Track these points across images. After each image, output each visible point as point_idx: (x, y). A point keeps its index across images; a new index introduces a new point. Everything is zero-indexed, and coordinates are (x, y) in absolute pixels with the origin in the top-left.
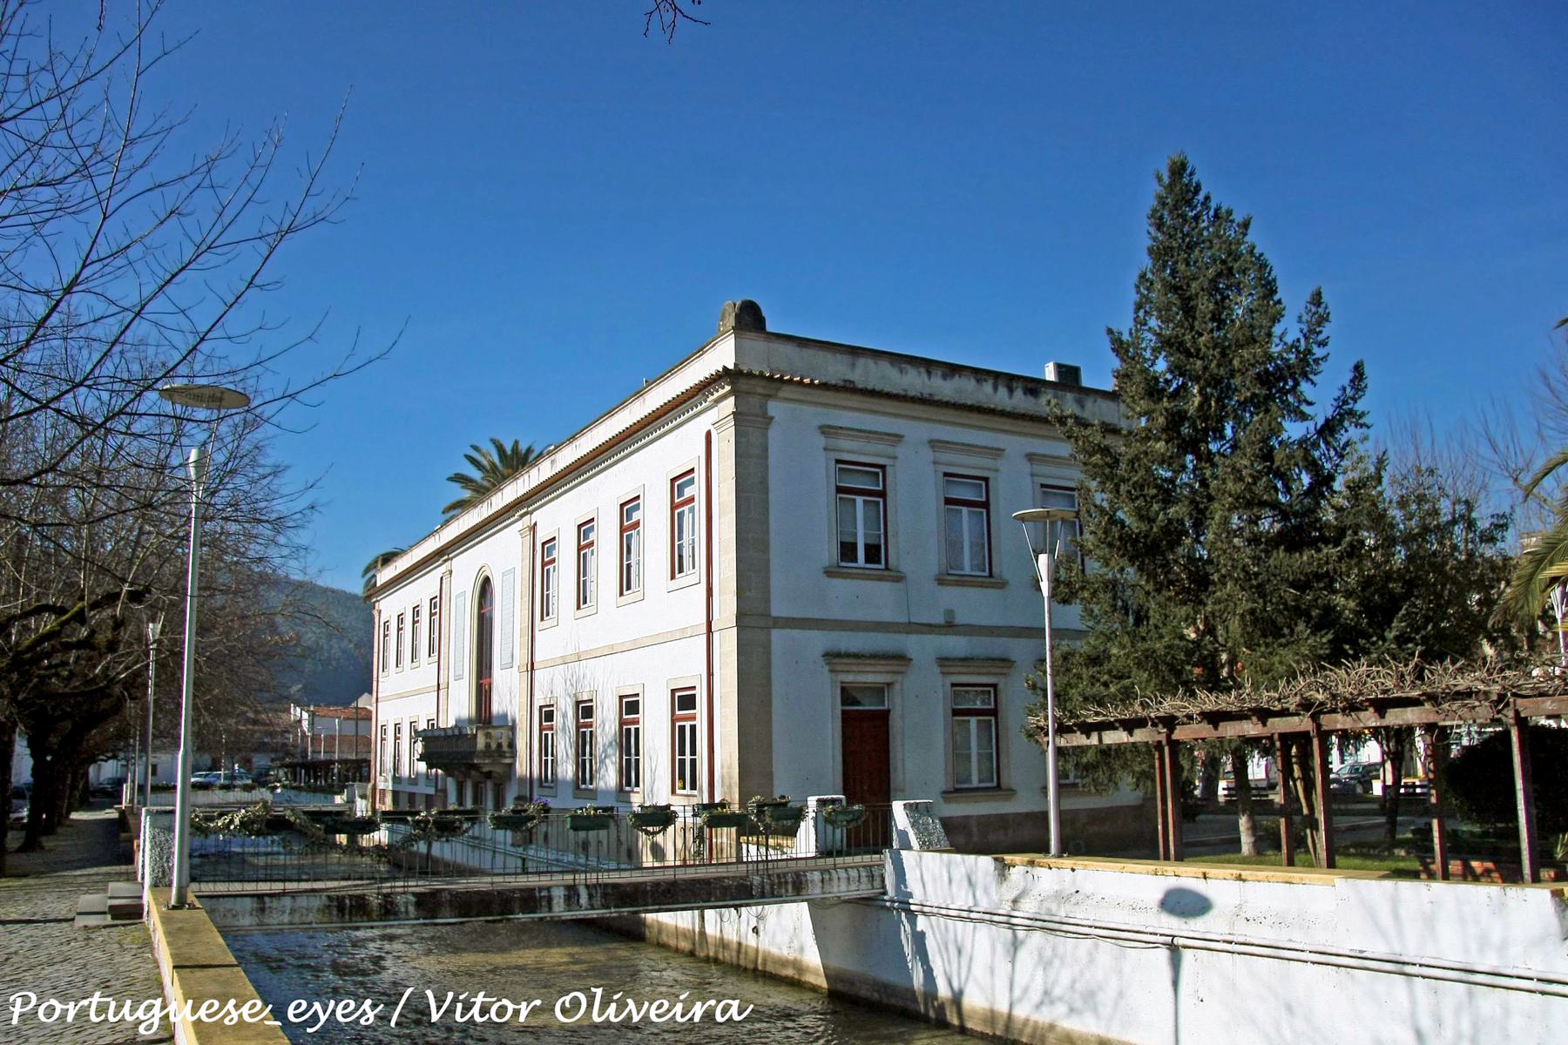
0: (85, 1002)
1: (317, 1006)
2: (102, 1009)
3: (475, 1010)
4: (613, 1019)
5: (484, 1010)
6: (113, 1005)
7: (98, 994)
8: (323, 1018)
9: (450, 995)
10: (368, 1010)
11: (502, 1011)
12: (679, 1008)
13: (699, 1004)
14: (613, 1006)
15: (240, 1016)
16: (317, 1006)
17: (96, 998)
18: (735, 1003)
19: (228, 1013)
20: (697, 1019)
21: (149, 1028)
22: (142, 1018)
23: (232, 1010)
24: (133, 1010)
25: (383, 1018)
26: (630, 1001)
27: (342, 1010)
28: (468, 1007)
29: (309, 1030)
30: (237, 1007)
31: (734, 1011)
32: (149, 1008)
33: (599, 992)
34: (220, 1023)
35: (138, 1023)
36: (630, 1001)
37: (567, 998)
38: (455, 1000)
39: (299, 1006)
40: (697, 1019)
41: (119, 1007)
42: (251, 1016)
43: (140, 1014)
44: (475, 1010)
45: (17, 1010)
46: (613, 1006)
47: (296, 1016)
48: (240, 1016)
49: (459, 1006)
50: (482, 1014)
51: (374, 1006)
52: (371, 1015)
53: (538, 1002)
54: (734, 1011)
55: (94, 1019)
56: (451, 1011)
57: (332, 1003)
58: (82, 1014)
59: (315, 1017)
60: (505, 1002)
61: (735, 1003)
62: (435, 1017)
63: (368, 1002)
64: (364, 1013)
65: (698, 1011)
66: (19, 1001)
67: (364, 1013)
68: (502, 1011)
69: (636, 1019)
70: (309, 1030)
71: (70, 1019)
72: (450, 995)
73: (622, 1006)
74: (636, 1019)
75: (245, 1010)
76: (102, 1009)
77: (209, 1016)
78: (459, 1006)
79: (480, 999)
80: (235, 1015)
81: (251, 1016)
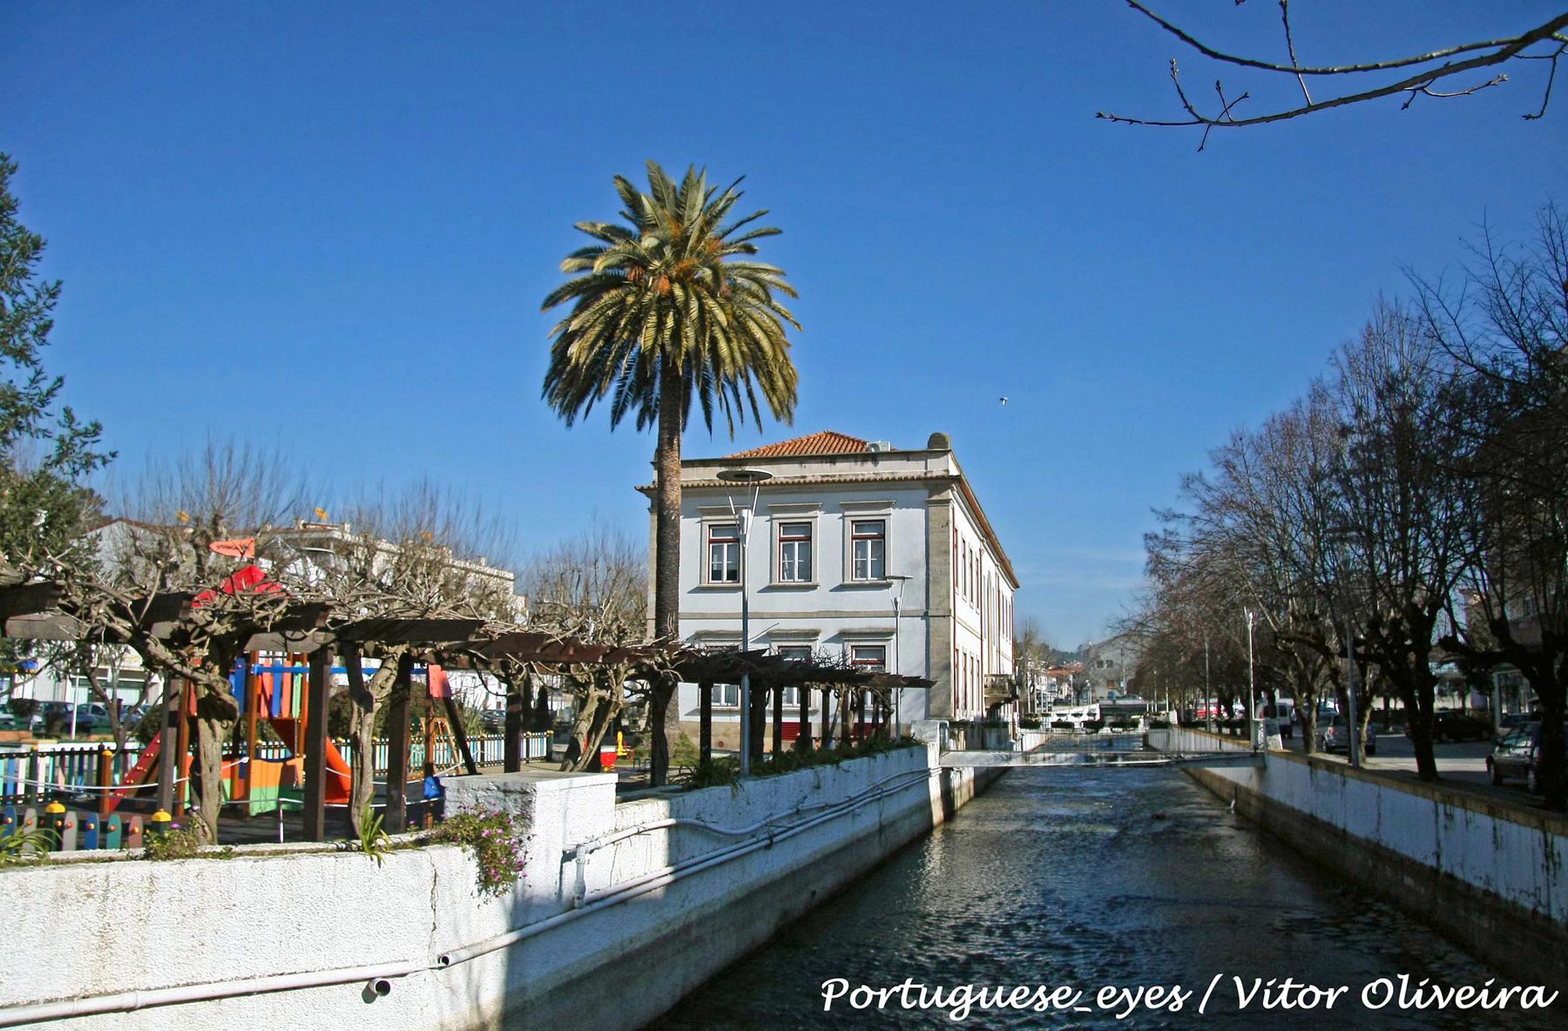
0: (897, 989)
1: (1126, 992)
3: (1283, 997)
5: (1293, 995)
8: (1132, 1005)
9: (1258, 981)
10: (1177, 997)
11: (1309, 998)
12: (1485, 994)
13: (1504, 990)
14: (1419, 993)
16: (1126, 992)
17: (908, 985)
20: (1502, 1006)
21: (960, 1014)
22: (954, 1004)
23: (1043, 997)
25: (1190, 1005)
26: (1436, 988)
27: (1151, 997)
28: (1276, 993)
29: (1119, 1017)
30: (1047, 993)
31: (1539, 997)
33: (1405, 978)
34: (1030, 1010)
35: (950, 1008)
36: (1436, 988)
37: (1374, 985)
38: (1263, 986)
40: (1502, 1006)
41: (929, 997)
42: (1061, 1002)
43: (951, 1000)
44: (1283, 997)
45: (829, 997)
46: (1419, 993)
49: (1267, 992)
51: (1181, 994)
52: (1180, 1002)
53: (1345, 989)
54: (1539, 997)
55: (905, 1005)
57: (1141, 989)
58: (894, 1000)
59: (1124, 1006)
60: (1313, 988)
61: (1540, 990)
62: (1243, 1004)
63: (1177, 988)
65: (1503, 997)
66: (831, 988)
67: (1173, 1000)
68: (1309, 998)
69: (1442, 1005)
71: (881, 1005)
72: (1258, 981)
73: (1428, 992)
75: (1055, 996)
76: (914, 994)
78: (1267, 992)
79: (1288, 985)
80: (1045, 1001)
81: (1061, 1002)
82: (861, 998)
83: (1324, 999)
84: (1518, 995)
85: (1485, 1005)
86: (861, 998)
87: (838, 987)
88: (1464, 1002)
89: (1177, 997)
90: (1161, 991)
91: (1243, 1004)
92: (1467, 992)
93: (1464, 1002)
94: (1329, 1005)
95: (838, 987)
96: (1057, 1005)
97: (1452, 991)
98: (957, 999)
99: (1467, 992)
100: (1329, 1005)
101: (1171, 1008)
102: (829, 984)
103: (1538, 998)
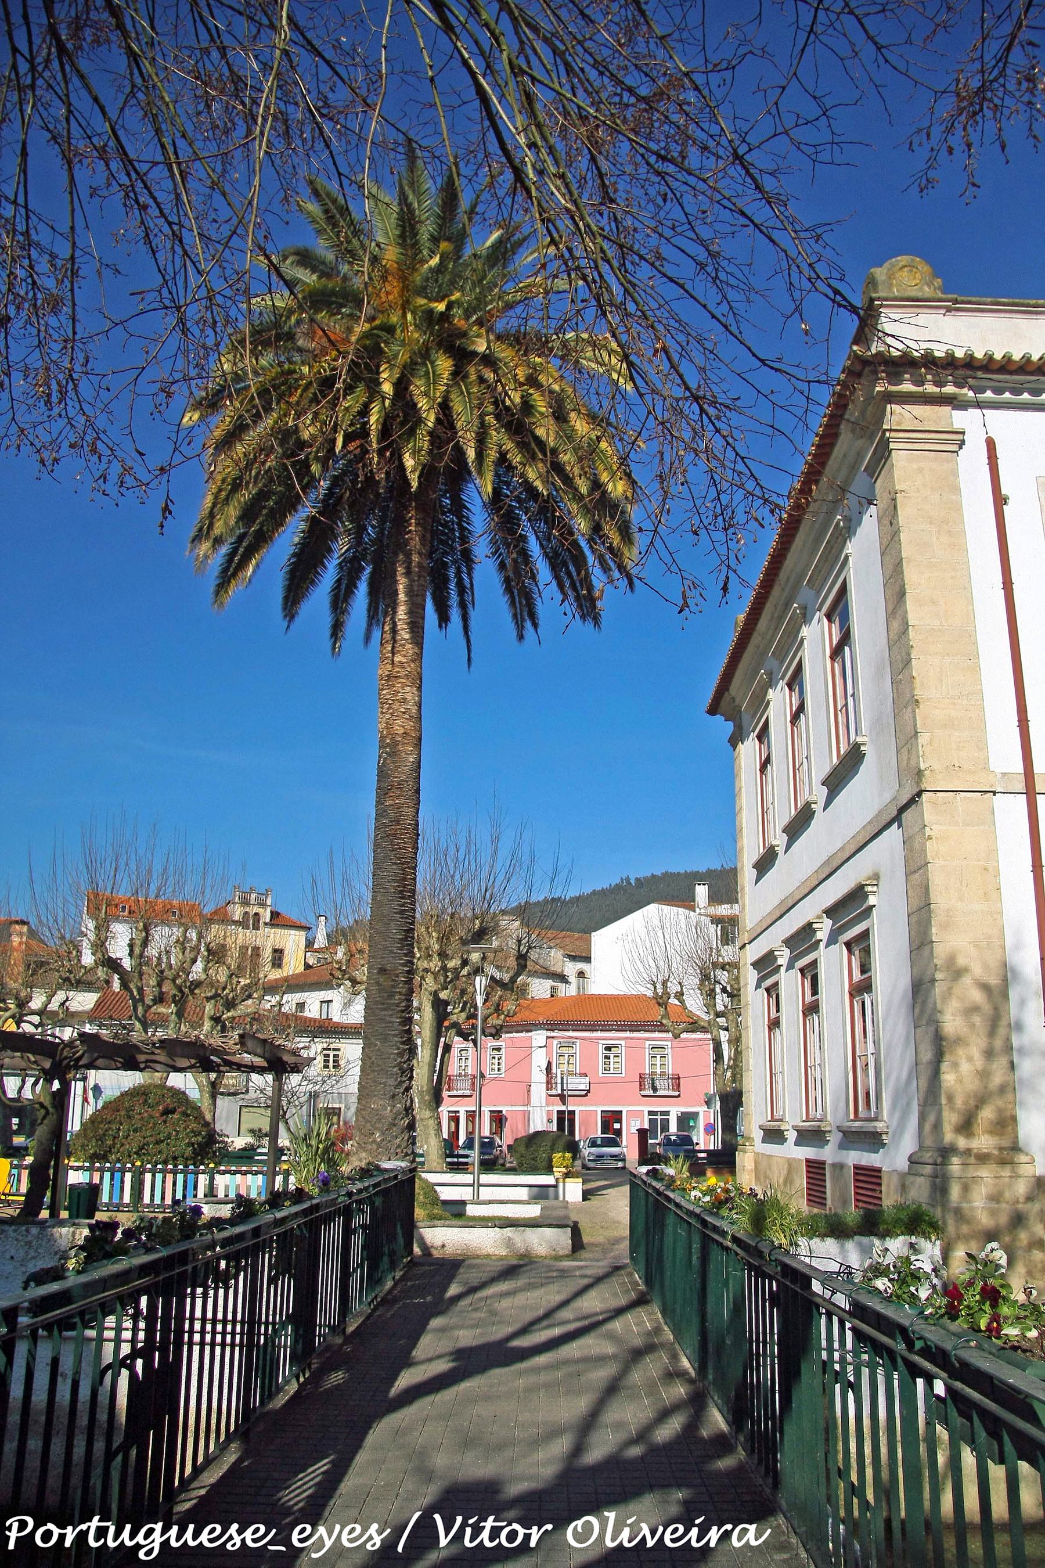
0: (84, 1527)
2: (101, 1533)
3: (485, 1535)
4: (626, 1544)
5: (495, 1533)
7: (97, 1518)
8: (328, 1543)
9: (459, 1519)
10: (375, 1535)
11: (512, 1536)
12: (694, 1532)
13: (715, 1529)
15: (243, 1540)
17: (95, 1522)
18: (752, 1528)
20: (712, 1544)
21: (148, 1553)
22: (142, 1542)
23: (235, 1535)
24: (133, 1535)
26: (644, 1526)
28: (477, 1531)
30: (240, 1532)
31: (751, 1535)
32: (150, 1531)
35: (138, 1547)
37: (579, 1523)
39: (303, 1530)
40: (712, 1544)
43: (140, 1538)
44: (485, 1535)
45: (13, 1535)
48: (243, 1540)
49: (468, 1530)
50: (492, 1539)
51: (380, 1532)
52: (378, 1540)
54: (751, 1535)
55: (92, 1543)
56: (460, 1536)
57: (338, 1527)
58: (83, 1536)
62: (443, 1542)
63: (375, 1527)
64: (371, 1538)
65: (714, 1535)
66: (16, 1526)
68: (512, 1536)
69: (650, 1543)
70: (314, 1556)
74: (650, 1543)
75: (248, 1534)
76: (101, 1533)
77: (211, 1541)
78: (468, 1530)
79: (490, 1523)
80: (237, 1540)
81: (254, 1541)
82: (47, 1536)
83: (62, 1537)
84: (727, 1535)
85: (694, 1544)
86: (47, 1536)
87: (23, 1525)
88: (673, 1541)
89: (375, 1535)
90: (219, 1529)
94: (68, 1544)
95: (23, 1525)
98: (146, 1537)
99: (353, 1530)
100: (68, 1544)
101: (229, 1546)
102: (13, 1522)
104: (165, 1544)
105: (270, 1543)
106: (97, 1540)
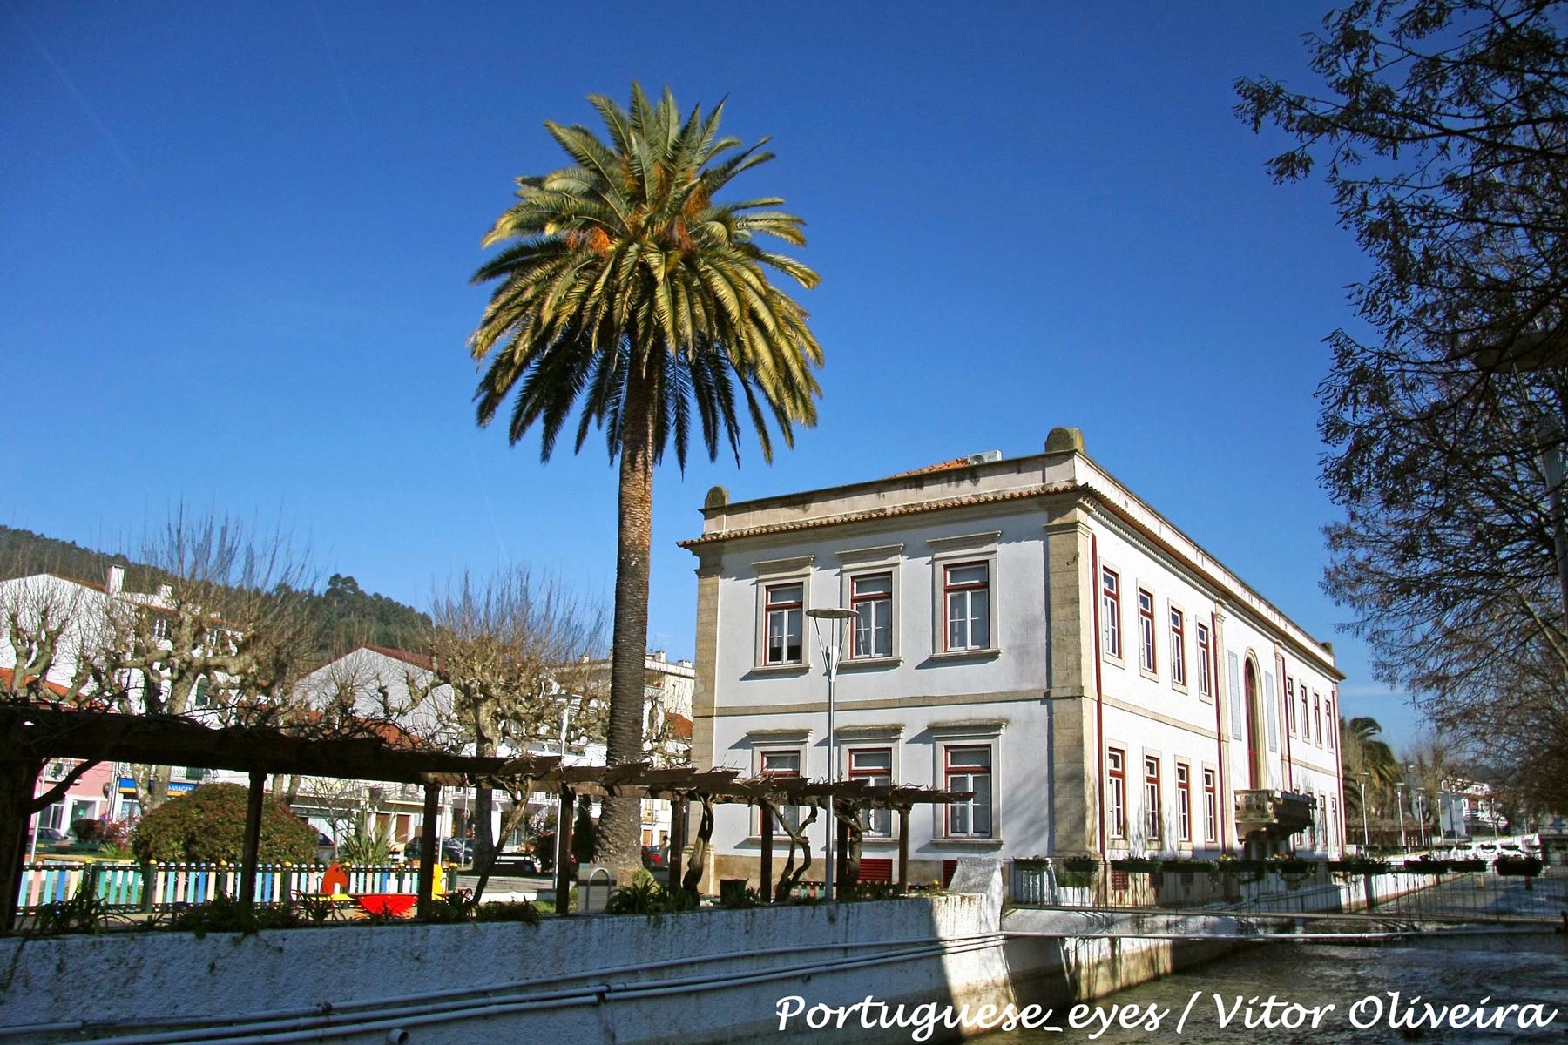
0: (856, 1007)
1: (1099, 1011)
3: (1266, 1016)
4: (1411, 1025)
6: (885, 1010)
7: (869, 998)
8: (1106, 1024)
9: (1240, 999)
10: (1153, 1015)
11: (1293, 1017)
12: (1480, 1012)
13: (1500, 1009)
14: (1411, 1011)
16: (1099, 1011)
17: (868, 1003)
18: (1539, 1008)
19: (1149, 1018)
20: (1498, 1025)
21: (922, 1034)
22: (916, 1023)
24: (906, 1016)
25: (1167, 1026)
26: (1428, 1006)
28: (1259, 1010)
29: (1091, 1037)
31: (1537, 1016)
32: (924, 1012)
33: (1395, 996)
35: (912, 1027)
36: (1428, 1006)
37: (1363, 1003)
38: (1245, 1004)
40: (1498, 1025)
41: (890, 1015)
42: (1031, 1021)
43: (913, 1019)
44: (1266, 1016)
45: (784, 1016)
46: (1411, 1011)
47: (1077, 1021)
49: (1249, 1011)
50: (1273, 1020)
51: (1158, 1013)
52: (1156, 1021)
53: (1332, 1007)
54: (1537, 1016)
55: (865, 1024)
57: (1116, 1008)
58: (855, 1017)
60: (1297, 1006)
61: (1539, 1008)
62: (1223, 1023)
63: (1153, 1007)
66: (786, 1006)
67: (1149, 1018)
68: (1293, 1017)
69: (1435, 1024)
70: (1091, 1037)
71: (840, 1024)
72: (1240, 999)
73: (1420, 1010)
74: (1435, 1024)
75: (1024, 1015)
76: (873, 1013)
78: (1249, 1011)
79: (1271, 1003)
81: (1031, 1021)
82: (819, 1016)
84: (1514, 1015)
85: (1480, 1025)
86: (819, 1016)
87: (794, 1006)
88: (1458, 1021)
89: (1153, 1015)
91: (1223, 1023)
92: (1461, 1010)
93: (1077, 1021)
95: (794, 1006)
96: (1026, 1024)
97: (1445, 1009)
98: (919, 1018)
102: (784, 1002)
103: (1537, 1018)
104: (939, 1025)
105: (1046, 1024)
106: (869, 1021)
